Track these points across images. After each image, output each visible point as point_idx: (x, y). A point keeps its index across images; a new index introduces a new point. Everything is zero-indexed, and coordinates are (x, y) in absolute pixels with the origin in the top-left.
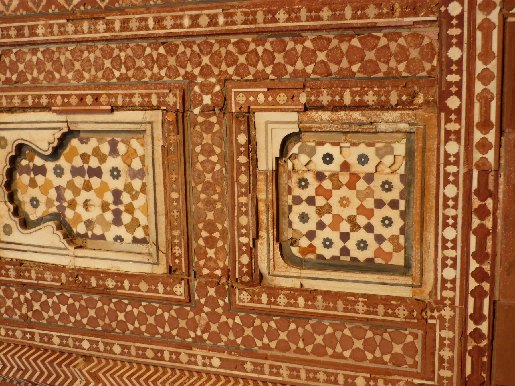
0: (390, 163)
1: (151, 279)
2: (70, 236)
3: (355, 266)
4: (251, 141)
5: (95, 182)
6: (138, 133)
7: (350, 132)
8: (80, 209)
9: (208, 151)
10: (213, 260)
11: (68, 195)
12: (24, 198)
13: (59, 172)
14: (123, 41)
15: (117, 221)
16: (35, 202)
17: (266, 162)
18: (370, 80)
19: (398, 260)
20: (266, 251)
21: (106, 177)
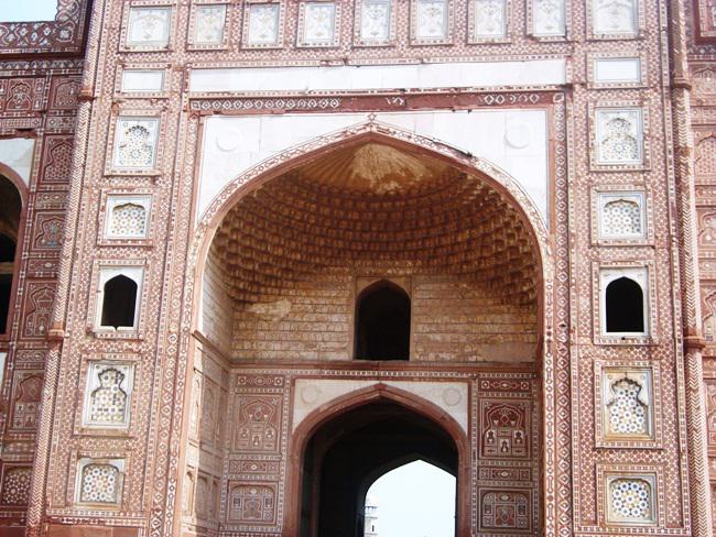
0: (109, 497)
1: (78, 423)
2: (95, 391)
3: (83, 486)
4: (116, 458)
5: (111, 402)
6: (123, 421)
7: (116, 487)
8: (103, 396)
9: (116, 444)
10: (85, 443)
11: (108, 392)
12: (108, 374)
13: (115, 389)
14: (149, 417)
15: (100, 410)
16: (106, 378)
17: (112, 462)
18: (130, 492)
19: (84, 499)
20: (85, 461)
21: (113, 407)
